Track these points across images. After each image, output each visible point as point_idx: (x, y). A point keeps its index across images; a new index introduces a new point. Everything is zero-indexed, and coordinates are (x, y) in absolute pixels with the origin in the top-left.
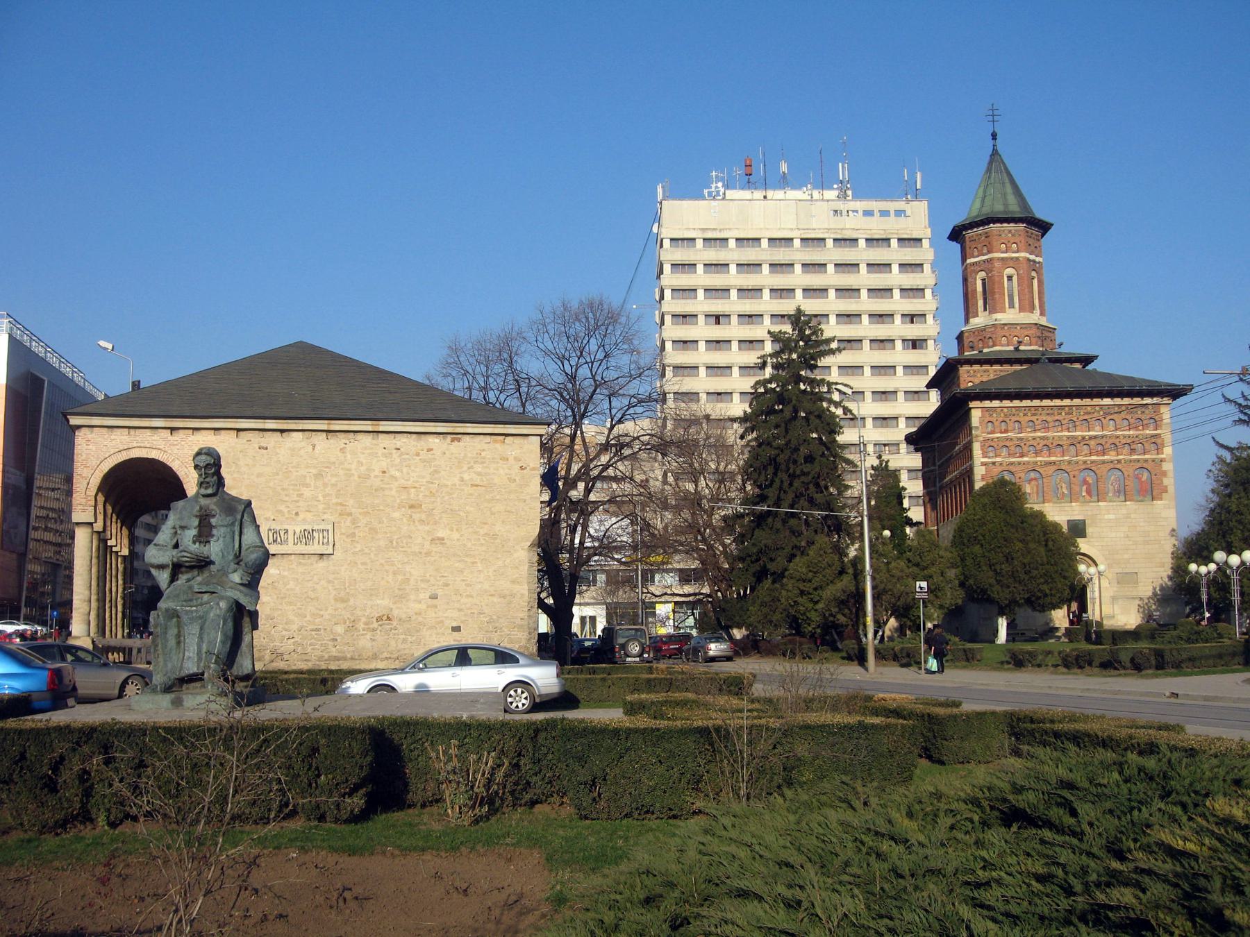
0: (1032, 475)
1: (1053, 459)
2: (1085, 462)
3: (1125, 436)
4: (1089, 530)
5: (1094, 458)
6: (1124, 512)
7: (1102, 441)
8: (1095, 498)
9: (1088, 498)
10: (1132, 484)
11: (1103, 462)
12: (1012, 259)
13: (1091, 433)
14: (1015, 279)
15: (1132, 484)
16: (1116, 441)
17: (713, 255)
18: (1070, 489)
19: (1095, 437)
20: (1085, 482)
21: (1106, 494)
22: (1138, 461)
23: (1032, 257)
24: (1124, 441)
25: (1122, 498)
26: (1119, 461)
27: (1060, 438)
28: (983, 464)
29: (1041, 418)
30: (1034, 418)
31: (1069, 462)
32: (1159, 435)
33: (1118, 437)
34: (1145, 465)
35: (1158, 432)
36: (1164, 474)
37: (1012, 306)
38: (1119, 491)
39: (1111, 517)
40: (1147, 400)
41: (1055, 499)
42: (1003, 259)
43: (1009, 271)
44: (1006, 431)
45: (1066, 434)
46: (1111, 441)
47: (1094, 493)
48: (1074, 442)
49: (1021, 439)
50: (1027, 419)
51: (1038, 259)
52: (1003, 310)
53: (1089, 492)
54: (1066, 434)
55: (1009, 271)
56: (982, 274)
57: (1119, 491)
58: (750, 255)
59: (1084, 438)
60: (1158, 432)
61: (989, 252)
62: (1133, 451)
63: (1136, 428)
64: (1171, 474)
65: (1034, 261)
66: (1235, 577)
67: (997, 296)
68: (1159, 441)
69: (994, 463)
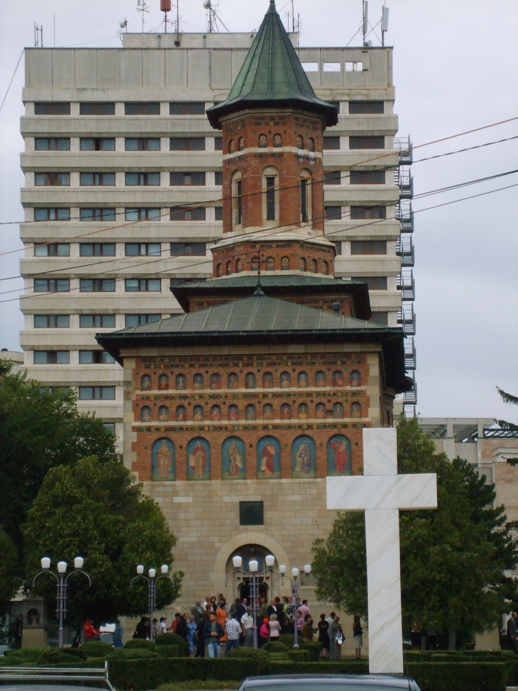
0: (198, 444)
1: (225, 422)
2: (265, 427)
3: (318, 394)
4: (268, 515)
5: (277, 421)
6: (314, 491)
7: (289, 401)
9: (269, 473)
10: (322, 455)
11: (290, 427)
12: (273, 155)
14: (277, 181)
15: (322, 455)
16: (307, 400)
17: (94, 124)
18: (244, 461)
20: (266, 452)
21: (293, 468)
22: (334, 426)
23: (301, 152)
24: (317, 400)
25: (312, 473)
26: (310, 427)
27: (235, 396)
28: (135, 429)
29: (212, 370)
30: (202, 371)
32: (363, 393)
33: (309, 394)
34: (343, 431)
35: (363, 388)
37: (271, 216)
38: (309, 465)
39: (297, 498)
40: (348, 348)
42: (260, 156)
43: (270, 172)
44: (167, 387)
45: (244, 390)
46: (300, 400)
47: (276, 466)
48: (252, 405)
49: (185, 397)
50: (194, 371)
51: (312, 154)
52: (258, 222)
53: (270, 466)
54: (244, 390)
55: (270, 172)
56: (238, 176)
57: (309, 465)
58: (144, 123)
59: (265, 395)
60: (363, 388)
61: (246, 146)
62: (329, 413)
63: (334, 384)
65: (307, 158)
66: (62, 584)
67: (250, 205)
68: (362, 400)
69: (149, 429)
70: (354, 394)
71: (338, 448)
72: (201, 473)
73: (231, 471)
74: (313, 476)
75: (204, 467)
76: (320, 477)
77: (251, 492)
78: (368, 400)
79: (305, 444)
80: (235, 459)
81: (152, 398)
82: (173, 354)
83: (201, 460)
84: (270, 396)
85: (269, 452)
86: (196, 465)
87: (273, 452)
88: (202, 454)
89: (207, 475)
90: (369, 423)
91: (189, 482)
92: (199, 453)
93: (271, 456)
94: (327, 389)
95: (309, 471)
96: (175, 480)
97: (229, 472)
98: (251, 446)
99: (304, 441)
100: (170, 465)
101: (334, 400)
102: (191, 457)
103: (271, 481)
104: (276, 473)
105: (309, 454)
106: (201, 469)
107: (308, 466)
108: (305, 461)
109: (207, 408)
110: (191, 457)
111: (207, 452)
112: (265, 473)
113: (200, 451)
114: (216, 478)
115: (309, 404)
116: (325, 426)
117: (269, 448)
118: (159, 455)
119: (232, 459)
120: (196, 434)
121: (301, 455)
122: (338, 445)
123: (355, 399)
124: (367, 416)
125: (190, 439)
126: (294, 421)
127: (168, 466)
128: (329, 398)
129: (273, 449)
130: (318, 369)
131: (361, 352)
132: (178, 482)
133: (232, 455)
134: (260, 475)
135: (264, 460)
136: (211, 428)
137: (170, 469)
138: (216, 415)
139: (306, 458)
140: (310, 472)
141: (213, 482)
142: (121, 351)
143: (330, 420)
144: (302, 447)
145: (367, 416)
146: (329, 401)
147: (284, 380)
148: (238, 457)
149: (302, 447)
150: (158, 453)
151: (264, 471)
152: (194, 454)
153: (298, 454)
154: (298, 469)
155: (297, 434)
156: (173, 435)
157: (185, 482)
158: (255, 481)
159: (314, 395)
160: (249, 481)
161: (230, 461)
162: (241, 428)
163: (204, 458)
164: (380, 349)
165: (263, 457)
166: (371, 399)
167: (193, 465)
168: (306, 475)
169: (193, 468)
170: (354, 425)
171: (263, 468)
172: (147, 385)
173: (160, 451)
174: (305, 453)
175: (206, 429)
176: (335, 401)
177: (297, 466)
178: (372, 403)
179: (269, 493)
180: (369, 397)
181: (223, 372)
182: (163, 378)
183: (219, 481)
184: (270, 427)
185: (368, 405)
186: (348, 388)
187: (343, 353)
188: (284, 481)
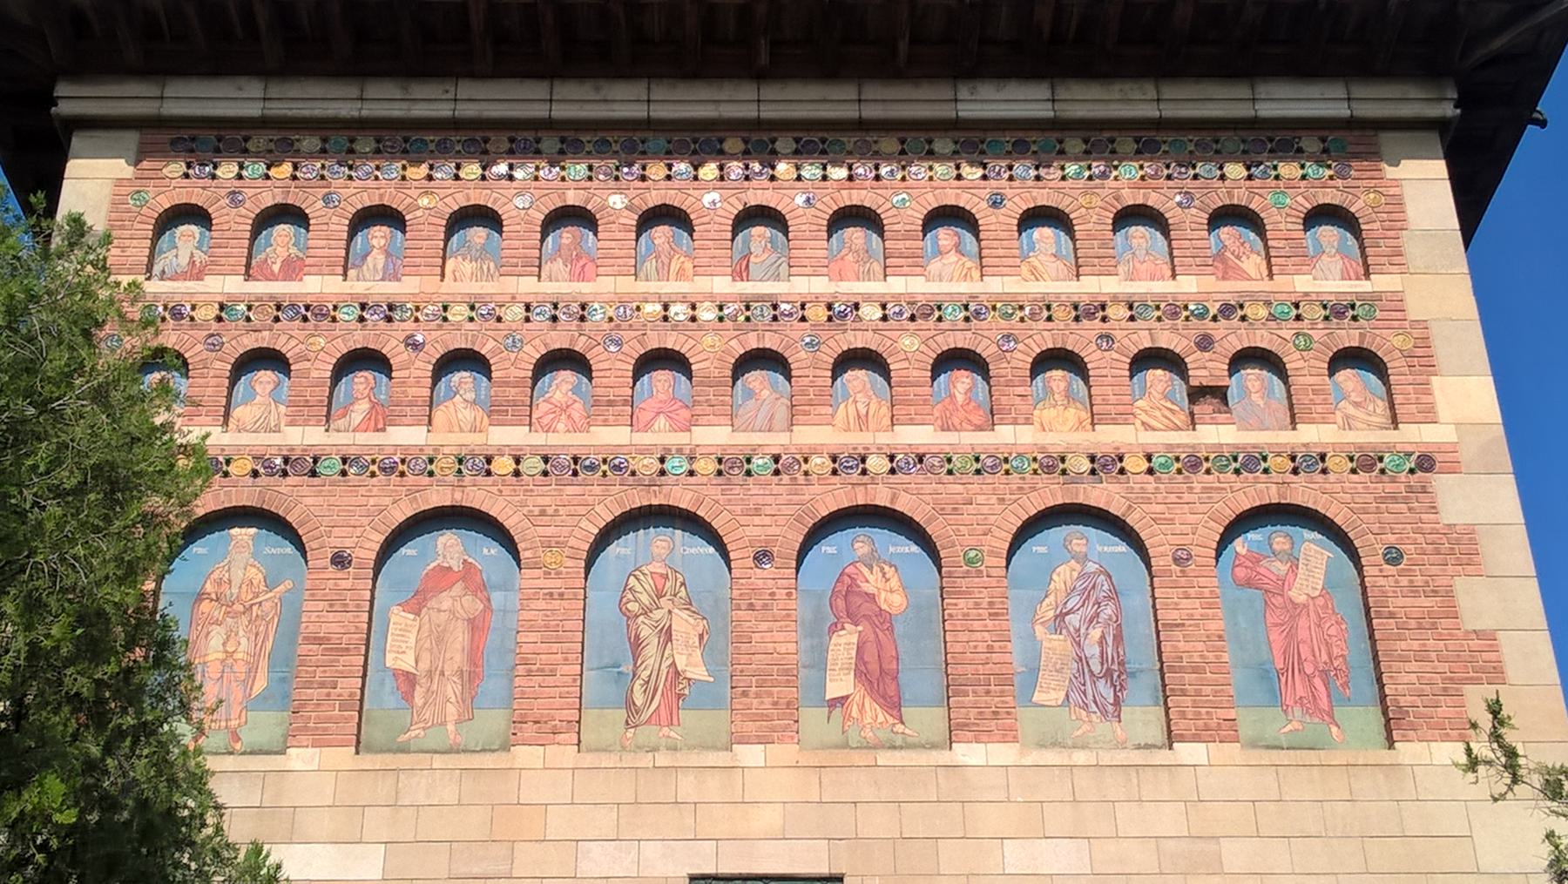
0: (449, 545)
6: (1168, 820)
8: (925, 719)
9: (872, 714)
13: (897, 285)
19: (928, 311)
20: (850, 601)
22: (1250, 462)
25: (1143, 719)
26: (1105, 465)
31: (732, 466)
33: (1094, 310)
35: (1380, 283)
36: (1462, 549)
38: (1117, 674)
41: (604, 723)
45: (723, 285)
47: (919, 678)
53: (880, 679)
60: (1380, 283)
63: (1222, 265)
64: (1511, 549)
68: (1388, 344)
70: (1337, 311)
71: (1283, 583)
72: (452, 710)
73: (639, 699)
74: (1157, 734)
75: (472, 676)
76: (1196, 739)
77: (767, 818)
78: (1425, 342)
79: (1083, 559)
80: (667, 635)
81: (207, 313)
82: (347, 110)
83: (459, 638)
84: (871, 312)
85: (871, 598)
86: (424, 665)
87: (893, 600)
88: (472, 605)
89: (493, 721)
90: (1453, 448)
91: (368, 761)
92: (453, 603)
93: (883, 620)
94: (1187, 285)
95: (1117, 703)
96: (283, 752)
97: (629, 704)
98: (762, 557)
99: (1078, 546)
100: (263, 664)
101: (1232, 338)
102: (399, 618)
103: (884, 758)
104: (925, 719)
105: (1108, 611)
106: (452, 689)
107: (1108, 674)
108: (1092, 650)
109: (513, 365)
110: (399, 618)
111: (497, 598)
112: (847, 717)
113: (458, 589)
114: (547, 732)
115: (1092, 357)
116: (1193, 463)
117: (871, 581)
118: (205, 606)
119: (645, 632)
120: (438, 497)
121: (1061, 616)
122: (1280, 568)
123: (1348, 337)
124: (1429, 415)
125: (401, 513)
126: (1005, 435)
127: (252, 671)
128: (1199, 327)
129: (894, 583)
130: (1130, 198)
131: (1351, 124)
132: (300, 758)
133: (646, 612)
134: (813, 719)
135: (844, 644)
136: (532, 465)
137: (260, 685)
138: (565, 409)
139: (1096, 633)
140: (1126, 711)
141: (525, 755)
142: (61, 90)
143: (1216, 434)
144: (1064, 575)
145: (1429, 415)
146: (1205, 343)
147: (939, 253)
148: (685, 625)
149: (1064, 575)
150: (200, 597)
151: (842, 700)
152: (416, 604)
153: (1047, 611)
154: (1050, 693)
155: (1034, 505)
156: (295, 499)
157: (344, 756)
158: (784, 752)
159: (1118, 312)
160: (751, 755)
161: (636, 645)
162: (706, 466)
163: (476, 626)
164: (1449, 110)
165: (834, 628)
166: (1436, 331)
167: (407, 663)
168: (1104, 728)
169: (408, 680)
170: (1366, 462)
171: (840, 684)
172: (184, 260)
173: (209, 587)
174: (1090, 610)
175: (503, 465)
176: (1236, 344)
177: (1044, 678)
178: (1442, 350)
179: (878, 823)
180: (1423, 325)
181: (617, 202)
182: (283, 231)
183: (564, 754)
184: (876, 464)
185: (1423, 359)
186: (1303, 283)
187: (1254, 123)
188: (968, 753)
